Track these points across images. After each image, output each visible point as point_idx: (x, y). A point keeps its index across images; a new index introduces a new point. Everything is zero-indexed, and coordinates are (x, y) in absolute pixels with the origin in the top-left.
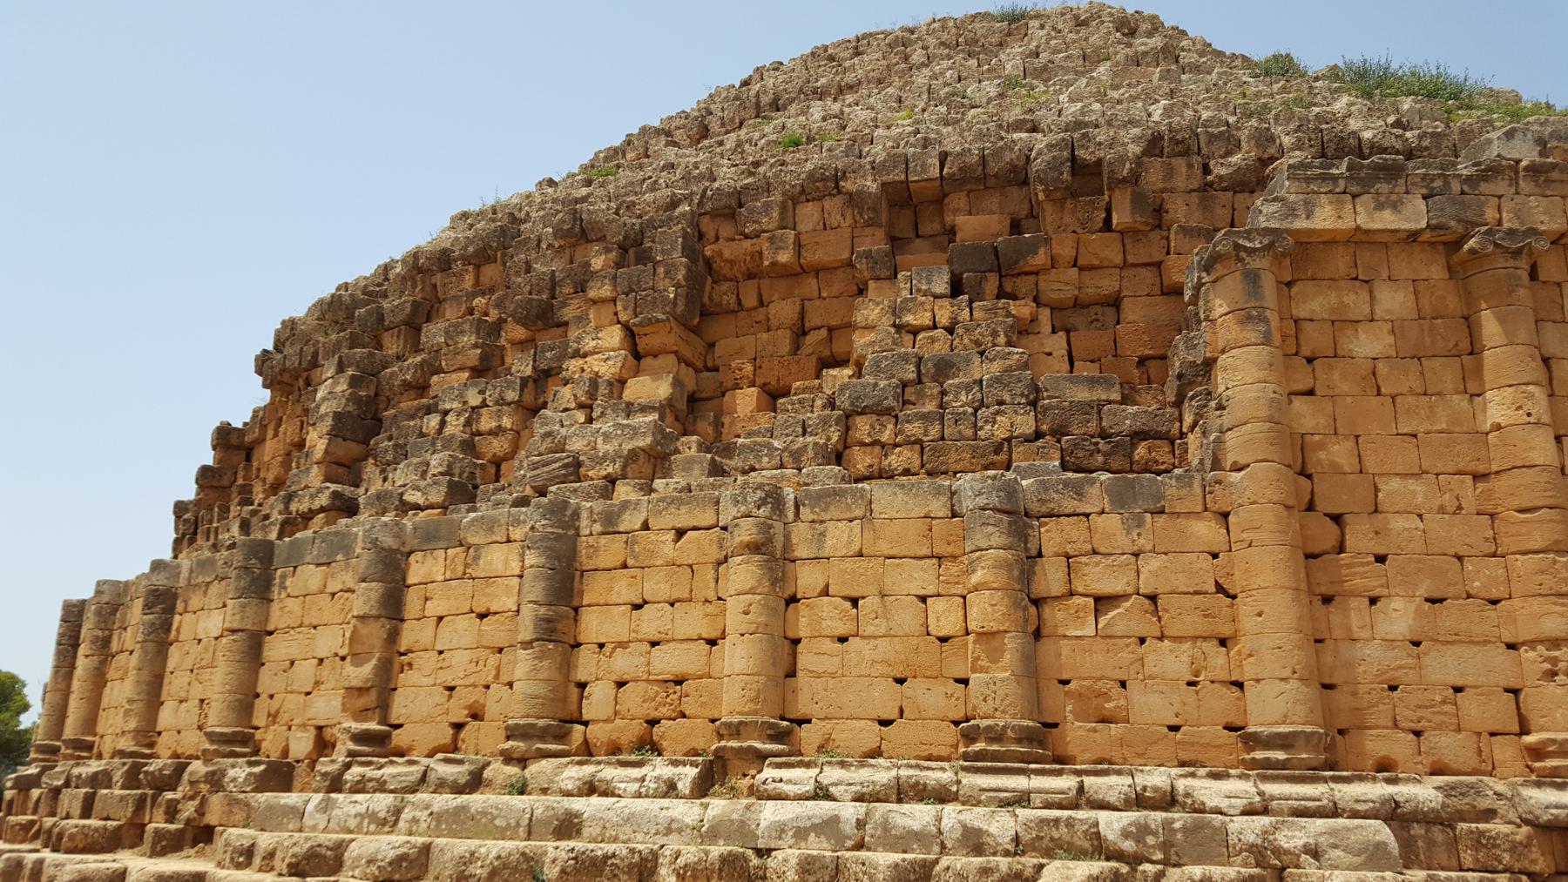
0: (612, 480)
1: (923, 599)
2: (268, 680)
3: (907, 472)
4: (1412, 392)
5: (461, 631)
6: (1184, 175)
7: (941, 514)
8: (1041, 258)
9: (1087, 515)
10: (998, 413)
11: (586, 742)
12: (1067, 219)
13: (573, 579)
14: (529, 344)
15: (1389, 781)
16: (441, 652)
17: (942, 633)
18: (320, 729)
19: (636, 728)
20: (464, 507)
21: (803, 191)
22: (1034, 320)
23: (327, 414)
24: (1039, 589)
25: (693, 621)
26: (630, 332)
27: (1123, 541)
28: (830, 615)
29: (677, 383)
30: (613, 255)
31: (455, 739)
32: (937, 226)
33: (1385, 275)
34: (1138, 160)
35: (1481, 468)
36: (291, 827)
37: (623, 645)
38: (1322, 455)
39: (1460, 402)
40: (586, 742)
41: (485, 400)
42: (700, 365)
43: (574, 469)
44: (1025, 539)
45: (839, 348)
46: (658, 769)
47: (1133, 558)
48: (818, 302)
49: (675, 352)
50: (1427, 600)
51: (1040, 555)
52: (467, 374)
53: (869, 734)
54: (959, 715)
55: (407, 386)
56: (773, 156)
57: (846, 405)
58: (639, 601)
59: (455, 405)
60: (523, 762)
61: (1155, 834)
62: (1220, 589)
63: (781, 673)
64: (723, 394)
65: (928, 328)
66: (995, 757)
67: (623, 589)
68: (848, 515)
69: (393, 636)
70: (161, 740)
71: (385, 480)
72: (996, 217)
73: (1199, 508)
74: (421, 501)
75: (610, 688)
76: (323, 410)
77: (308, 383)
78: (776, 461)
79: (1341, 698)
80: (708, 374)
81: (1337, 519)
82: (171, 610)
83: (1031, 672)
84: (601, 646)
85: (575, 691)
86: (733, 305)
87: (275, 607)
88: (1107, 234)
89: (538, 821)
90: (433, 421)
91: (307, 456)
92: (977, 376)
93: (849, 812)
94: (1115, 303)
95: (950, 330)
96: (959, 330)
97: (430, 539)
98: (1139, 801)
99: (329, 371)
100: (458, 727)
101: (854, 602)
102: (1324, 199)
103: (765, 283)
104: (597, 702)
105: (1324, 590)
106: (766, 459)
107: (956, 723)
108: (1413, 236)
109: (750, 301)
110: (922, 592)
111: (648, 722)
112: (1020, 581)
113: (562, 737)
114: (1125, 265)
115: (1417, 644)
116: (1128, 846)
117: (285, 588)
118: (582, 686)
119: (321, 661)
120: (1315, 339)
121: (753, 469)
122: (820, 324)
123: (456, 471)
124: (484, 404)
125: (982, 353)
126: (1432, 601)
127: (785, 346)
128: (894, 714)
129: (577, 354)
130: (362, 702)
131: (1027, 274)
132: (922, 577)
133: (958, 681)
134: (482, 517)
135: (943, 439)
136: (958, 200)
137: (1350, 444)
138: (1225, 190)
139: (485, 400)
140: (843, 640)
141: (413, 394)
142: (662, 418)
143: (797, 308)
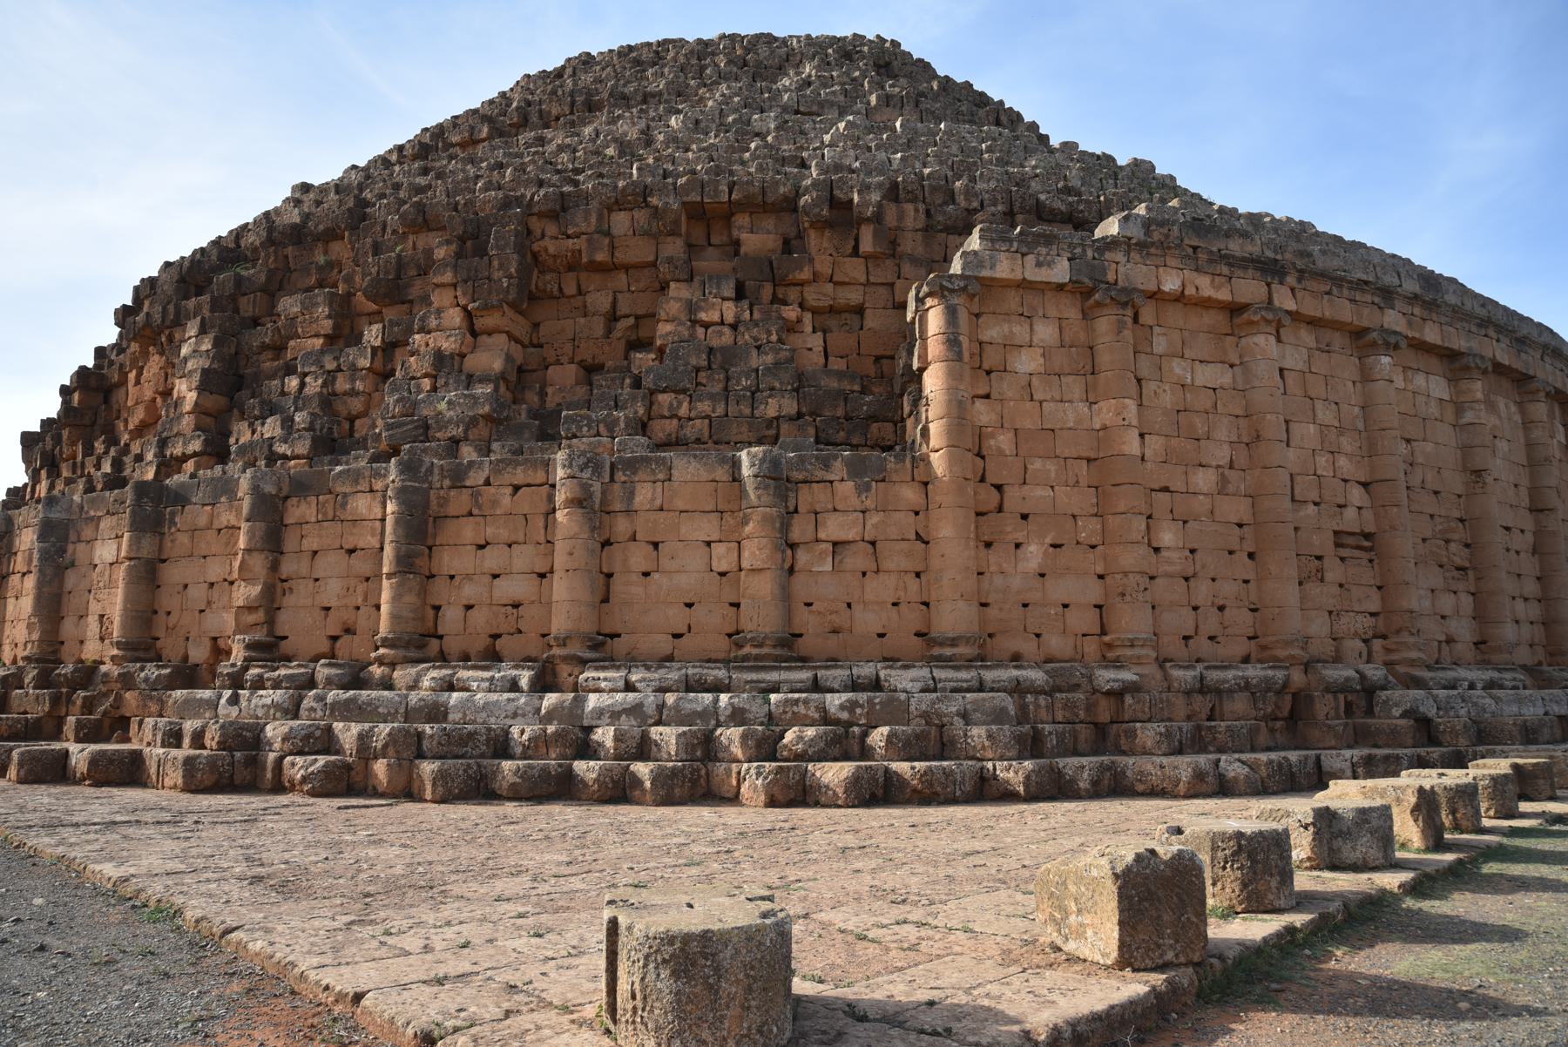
0: (455, 442)
1: (708, 544)
2: (167, 600)
3: (698, 441)
4: (1053, 400)
6: (912, 216)
7: (724, 479)
8: (805, 274)
9: (831, 482)
10: (770, 396)
11: (441, 651)
12: (825, 244)
13: (426, 522)
14: (377, 318)
15: (1016, 667)
16: (317, 580)
17: (721, 570)
18: (215, 639)
19: (482, 642)
20: (327, 459)
21: (617, 202)
22: (799, 321)
23: (195, 370)
24: (795, 535)
25: (524, 558)
26: (469, 315)
27: (855, 502)
28: (638, 557)
29: (509, 358)
30: (453, 247)
31: (333, 649)
32: (725, 238)
33: (1041, 314)
34: (879, 205)
35: (1093, 455)
36: (207, 715)
37: (468, 577)
38: (992, 442)
39: (1083, 408)
40: (441, 651)
41: (339, 365)
42: (526, 341)
43: (424, 430)
44: (785, 499)
45: (643, 333)
46: (506, 671)
47: (861, 515)
48: (627, 295)
49: (507, 332)
50: (1052, 545)
51: (796, 511)
52: (321, 341)
53: (664, 644)
54: (731, 630)
55: (264, 347)
56: (591, 167)
57: (651, 386)
58: (483, 542)
60: (393, 665)
61: (862, 706)
62: (918, 537)
63: (598, 600)
64: (547, 368)
65: (717, 324)
66: (757, 658)
67: (468, 531)
68: (652, 478)
69: (274, 567)
70: (65, 648)
71: (253, 433)
72: (772, 236)
73: (909, 478)
74: (289, 453)
75: (460, 612)
76: (190, 365)
77: (170, 339)
78: (594, 432)
79: (992, 612)
80: (533, 350)
81: (999, 488)
82: (65, 539)
83: (786, 595)
84: (452, 577)
85: (431, 613)
86: (556, 292)
87: (167, 539)
88: (855, 259)
89: (414, 709)
90: (293, 383)
91: (176, 407)
92: (755, 366)
93: (650, 699)
94: (859, 311)
95: (734, 327)
96: (741, 329)
97: (300, 488)
98: (854, 686)
99: (192, 329)
100: (334, 639)
101: (656, 545)
102: (1002, 256)
103: (583, 276)
104: (451, 618)
105: (986, 538)
106: (585, 429)
107: (730, 635)
108: (1060, 287)
109: (570, 289)
110: (708, 539)
111: (491, 636)
112: (781, 531)
113: (421, 647)
114: (868, 283)
115: (1042, 575)
116: (845, 716)
117: (175, 524)
118: (437, 608)
119: (212, 584)
120: (991, 358)
121: (575, 436)
122: (628, 312)
123: (318, 427)
124: (339, 370)
125: (758, 348)
126: (1054, 546)
127: (599, 330)
128: (684, 629)
129: (424, 330)
130: (251, 618)
131: (795, 285)
132: (707, 528)
133: (732, 605)
134: (349, 470)
135: (727, 415)
136: (742, 220)
137: (1011, 435)
138: (941, 231)
139: (339, 365)
140: (646, 574)
141: (270, 354)
142: (496, 389)
143: (610, 299)
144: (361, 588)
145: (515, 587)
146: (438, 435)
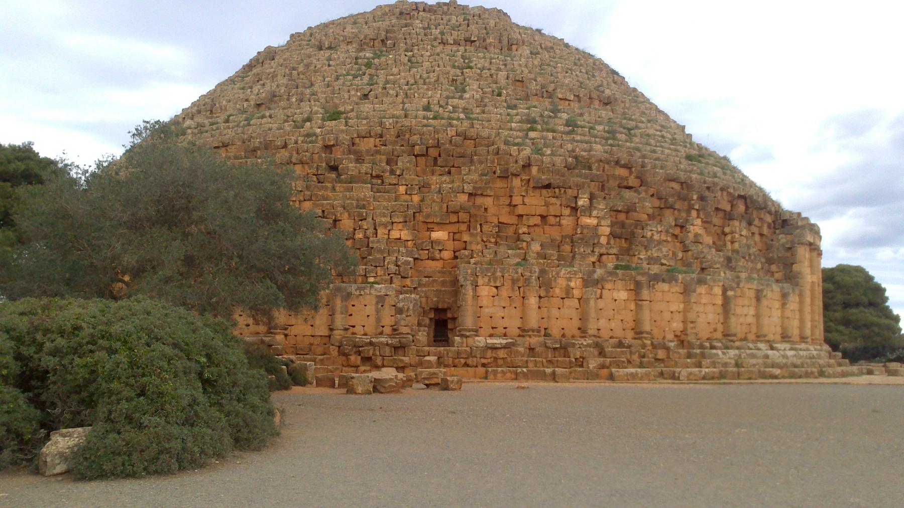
5: (710, 308)
18: (674, 331)
59: (655, 229)
67: (740, 301)
74: (668, 264)
119: (672, 312)
124: (661, 231)
144: (717, 317)
145: (750, 319)
146: (715, 266)
